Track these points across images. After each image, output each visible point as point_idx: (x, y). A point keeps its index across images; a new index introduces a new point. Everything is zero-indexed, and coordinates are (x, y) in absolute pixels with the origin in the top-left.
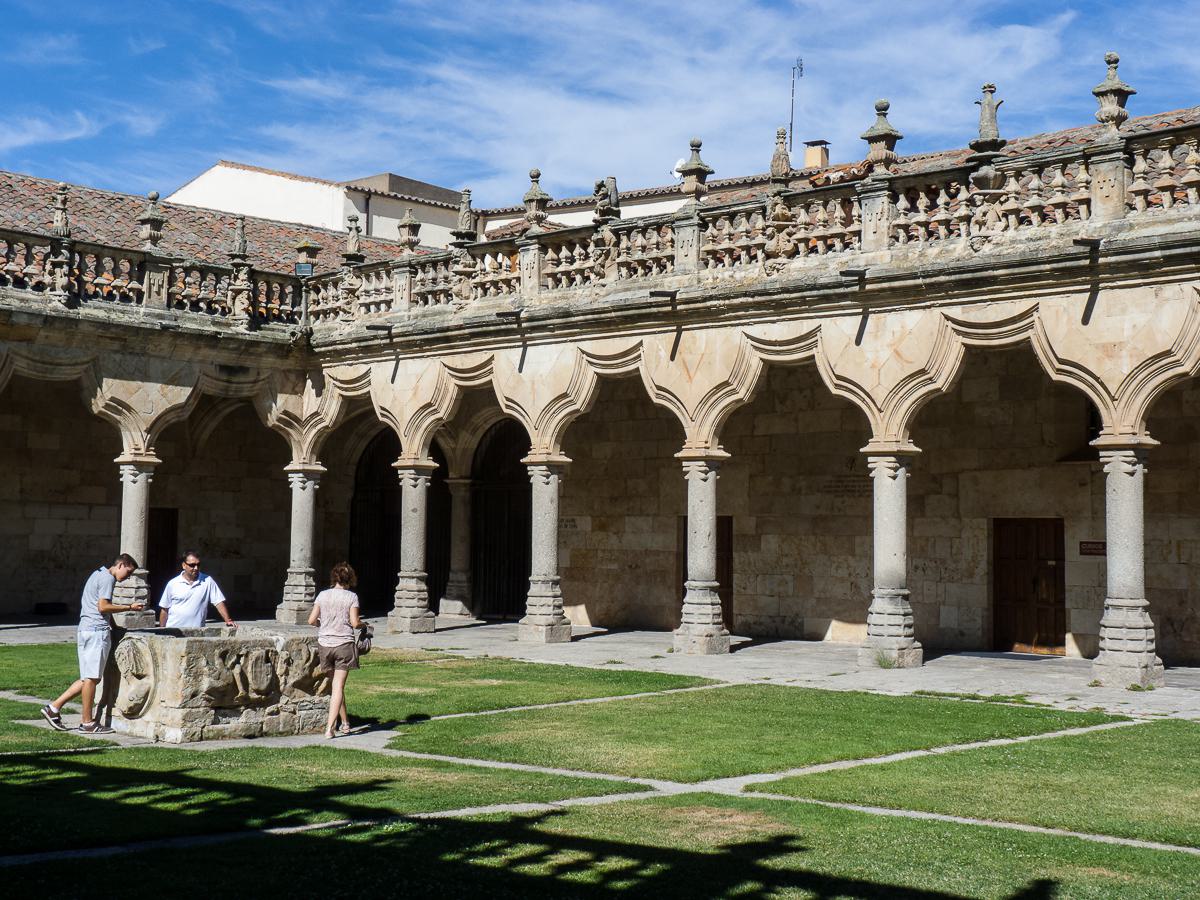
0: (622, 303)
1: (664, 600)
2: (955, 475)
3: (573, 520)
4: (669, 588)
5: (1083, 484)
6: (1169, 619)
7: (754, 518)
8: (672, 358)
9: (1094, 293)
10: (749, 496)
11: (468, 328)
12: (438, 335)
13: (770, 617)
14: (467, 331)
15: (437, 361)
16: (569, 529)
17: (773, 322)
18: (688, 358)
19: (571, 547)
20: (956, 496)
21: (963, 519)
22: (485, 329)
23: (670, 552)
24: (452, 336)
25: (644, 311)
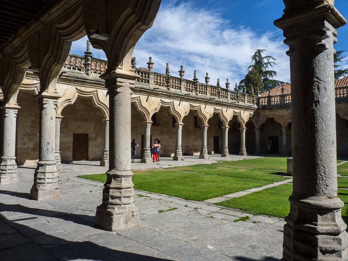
0: (142, 87)
1: (69, 154)
2: (137, 127)
3: (35, 134)
4: (71, 151)
5: (155, 130)
6: (165, 150)
7: (95, 134)
8: (147, 101)
9: (206, 105)
10: (94, 129)
11: (94, 81)
12: (82, 80)
13: (99, 156)
14: (93, 82)
15: (74, 87)
16: (33, 136)
17: (166, 98)
18: (150, 102)
19: (35, 142)
20: (137, 131)
21: (138, 135)
22: (100, 83)
23: (71, 142)
24: (86, 82)
25: (146, 90)
